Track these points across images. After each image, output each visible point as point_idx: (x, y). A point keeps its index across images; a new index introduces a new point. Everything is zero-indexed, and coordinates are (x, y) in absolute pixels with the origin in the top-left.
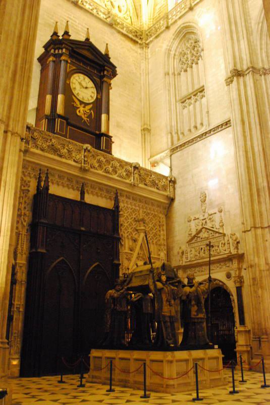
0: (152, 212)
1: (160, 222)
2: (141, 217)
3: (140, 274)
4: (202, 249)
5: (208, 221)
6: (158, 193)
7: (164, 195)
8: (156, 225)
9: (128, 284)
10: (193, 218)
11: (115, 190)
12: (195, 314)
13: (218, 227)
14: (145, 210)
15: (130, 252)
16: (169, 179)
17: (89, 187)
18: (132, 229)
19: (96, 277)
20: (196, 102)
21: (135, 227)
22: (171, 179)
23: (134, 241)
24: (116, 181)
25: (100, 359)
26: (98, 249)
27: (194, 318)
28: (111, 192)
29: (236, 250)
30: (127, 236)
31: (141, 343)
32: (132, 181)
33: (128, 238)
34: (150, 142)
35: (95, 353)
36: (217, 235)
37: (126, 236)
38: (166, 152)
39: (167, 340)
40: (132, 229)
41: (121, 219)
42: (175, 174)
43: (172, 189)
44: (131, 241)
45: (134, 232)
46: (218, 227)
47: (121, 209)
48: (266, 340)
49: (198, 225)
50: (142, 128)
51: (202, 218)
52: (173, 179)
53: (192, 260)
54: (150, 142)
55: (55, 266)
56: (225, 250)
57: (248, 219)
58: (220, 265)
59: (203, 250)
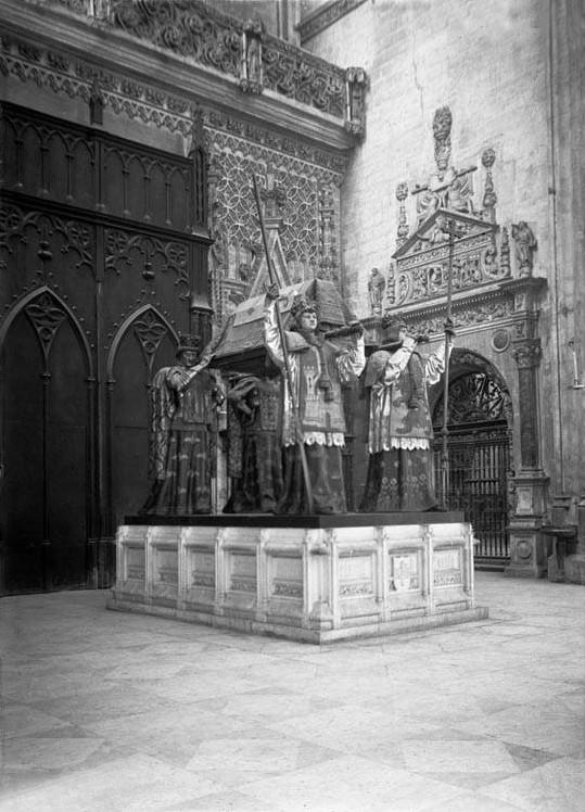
4: (432, 271)
5: (452, 195)
9: (214, 350)
10: (412, 188)
13: (479, 208)
15: (240, 281)
19: (144, 344)
23: (253, 253)
28: (182, 111)
29: (526, 269)
31: (247, 508)
36: (476, 230)
46: (479, 208)
47: (214, 162)
49: (424, 207)
51: (435, 185)
52: (361, 79)
53: (405, 302)
55: (23, 312)
56: (495, 272)
57: (568, 174)
58: (480, 312)
59: (434, 276)
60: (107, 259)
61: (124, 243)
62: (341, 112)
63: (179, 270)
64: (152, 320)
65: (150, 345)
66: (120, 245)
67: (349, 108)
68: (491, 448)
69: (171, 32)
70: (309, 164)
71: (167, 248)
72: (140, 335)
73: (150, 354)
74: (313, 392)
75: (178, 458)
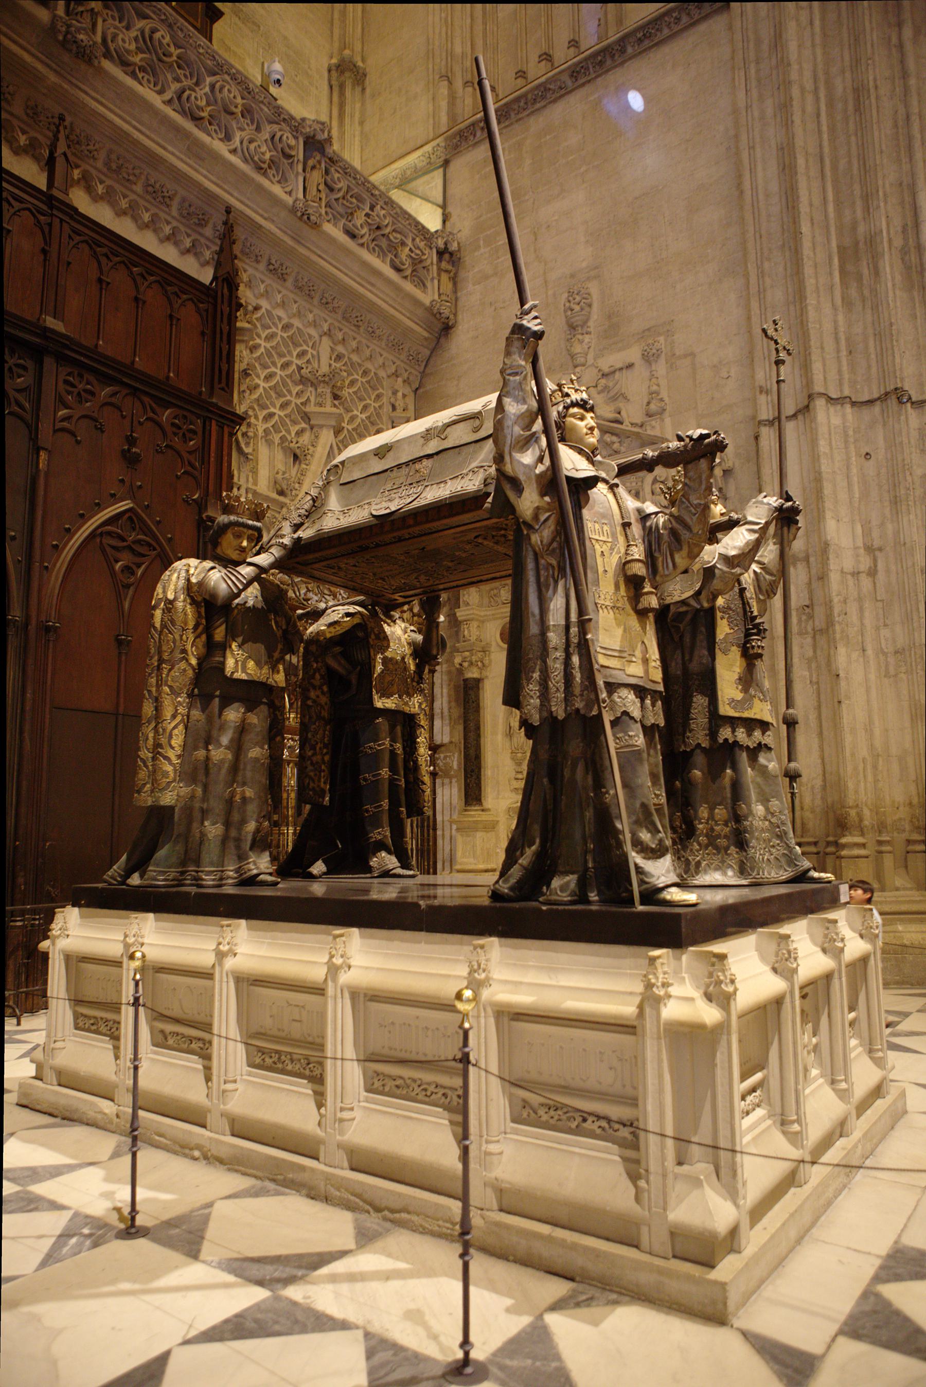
0: (368, 365)
1: (394, 408)
2: (324, 369)
3: (377, 466)
6: (398, 289)
7: (417, 302)
8: (378, 415)
9: (297, 527)
11: (218, 218)
12: (739, 696)
14: (340, 349)
15: (274, 495)
16: (440, 243)
17: (100, 164)
18: (288, 411)
21: (299, 402)
22: (446, 244)
23: (296, 457)
25: (24, 1102)
26: (131, 441)
27: (733, 722)
32: (301, 196)
33: (269, 443)
34: (361, 123)
35: (76, 932)
37: (261, 432)
38: (428, 148)
39: (639, 860)
40: (288, 411)
41: (243, 355)
42: (463, 227)
43: (447, 286)
44: (279, 456)
45: (295, 422)
48: (862, 852)
54: (361, 123)
60: (62, 413)
61: (93, 394)
62: (424, 285)
63: (186, 456)
64: (134, 529)
65: (127, 569)
67: (436, 282)
70: (378, 350)
72: (108, 549)
73: (127, 586)
74: (611, 589)
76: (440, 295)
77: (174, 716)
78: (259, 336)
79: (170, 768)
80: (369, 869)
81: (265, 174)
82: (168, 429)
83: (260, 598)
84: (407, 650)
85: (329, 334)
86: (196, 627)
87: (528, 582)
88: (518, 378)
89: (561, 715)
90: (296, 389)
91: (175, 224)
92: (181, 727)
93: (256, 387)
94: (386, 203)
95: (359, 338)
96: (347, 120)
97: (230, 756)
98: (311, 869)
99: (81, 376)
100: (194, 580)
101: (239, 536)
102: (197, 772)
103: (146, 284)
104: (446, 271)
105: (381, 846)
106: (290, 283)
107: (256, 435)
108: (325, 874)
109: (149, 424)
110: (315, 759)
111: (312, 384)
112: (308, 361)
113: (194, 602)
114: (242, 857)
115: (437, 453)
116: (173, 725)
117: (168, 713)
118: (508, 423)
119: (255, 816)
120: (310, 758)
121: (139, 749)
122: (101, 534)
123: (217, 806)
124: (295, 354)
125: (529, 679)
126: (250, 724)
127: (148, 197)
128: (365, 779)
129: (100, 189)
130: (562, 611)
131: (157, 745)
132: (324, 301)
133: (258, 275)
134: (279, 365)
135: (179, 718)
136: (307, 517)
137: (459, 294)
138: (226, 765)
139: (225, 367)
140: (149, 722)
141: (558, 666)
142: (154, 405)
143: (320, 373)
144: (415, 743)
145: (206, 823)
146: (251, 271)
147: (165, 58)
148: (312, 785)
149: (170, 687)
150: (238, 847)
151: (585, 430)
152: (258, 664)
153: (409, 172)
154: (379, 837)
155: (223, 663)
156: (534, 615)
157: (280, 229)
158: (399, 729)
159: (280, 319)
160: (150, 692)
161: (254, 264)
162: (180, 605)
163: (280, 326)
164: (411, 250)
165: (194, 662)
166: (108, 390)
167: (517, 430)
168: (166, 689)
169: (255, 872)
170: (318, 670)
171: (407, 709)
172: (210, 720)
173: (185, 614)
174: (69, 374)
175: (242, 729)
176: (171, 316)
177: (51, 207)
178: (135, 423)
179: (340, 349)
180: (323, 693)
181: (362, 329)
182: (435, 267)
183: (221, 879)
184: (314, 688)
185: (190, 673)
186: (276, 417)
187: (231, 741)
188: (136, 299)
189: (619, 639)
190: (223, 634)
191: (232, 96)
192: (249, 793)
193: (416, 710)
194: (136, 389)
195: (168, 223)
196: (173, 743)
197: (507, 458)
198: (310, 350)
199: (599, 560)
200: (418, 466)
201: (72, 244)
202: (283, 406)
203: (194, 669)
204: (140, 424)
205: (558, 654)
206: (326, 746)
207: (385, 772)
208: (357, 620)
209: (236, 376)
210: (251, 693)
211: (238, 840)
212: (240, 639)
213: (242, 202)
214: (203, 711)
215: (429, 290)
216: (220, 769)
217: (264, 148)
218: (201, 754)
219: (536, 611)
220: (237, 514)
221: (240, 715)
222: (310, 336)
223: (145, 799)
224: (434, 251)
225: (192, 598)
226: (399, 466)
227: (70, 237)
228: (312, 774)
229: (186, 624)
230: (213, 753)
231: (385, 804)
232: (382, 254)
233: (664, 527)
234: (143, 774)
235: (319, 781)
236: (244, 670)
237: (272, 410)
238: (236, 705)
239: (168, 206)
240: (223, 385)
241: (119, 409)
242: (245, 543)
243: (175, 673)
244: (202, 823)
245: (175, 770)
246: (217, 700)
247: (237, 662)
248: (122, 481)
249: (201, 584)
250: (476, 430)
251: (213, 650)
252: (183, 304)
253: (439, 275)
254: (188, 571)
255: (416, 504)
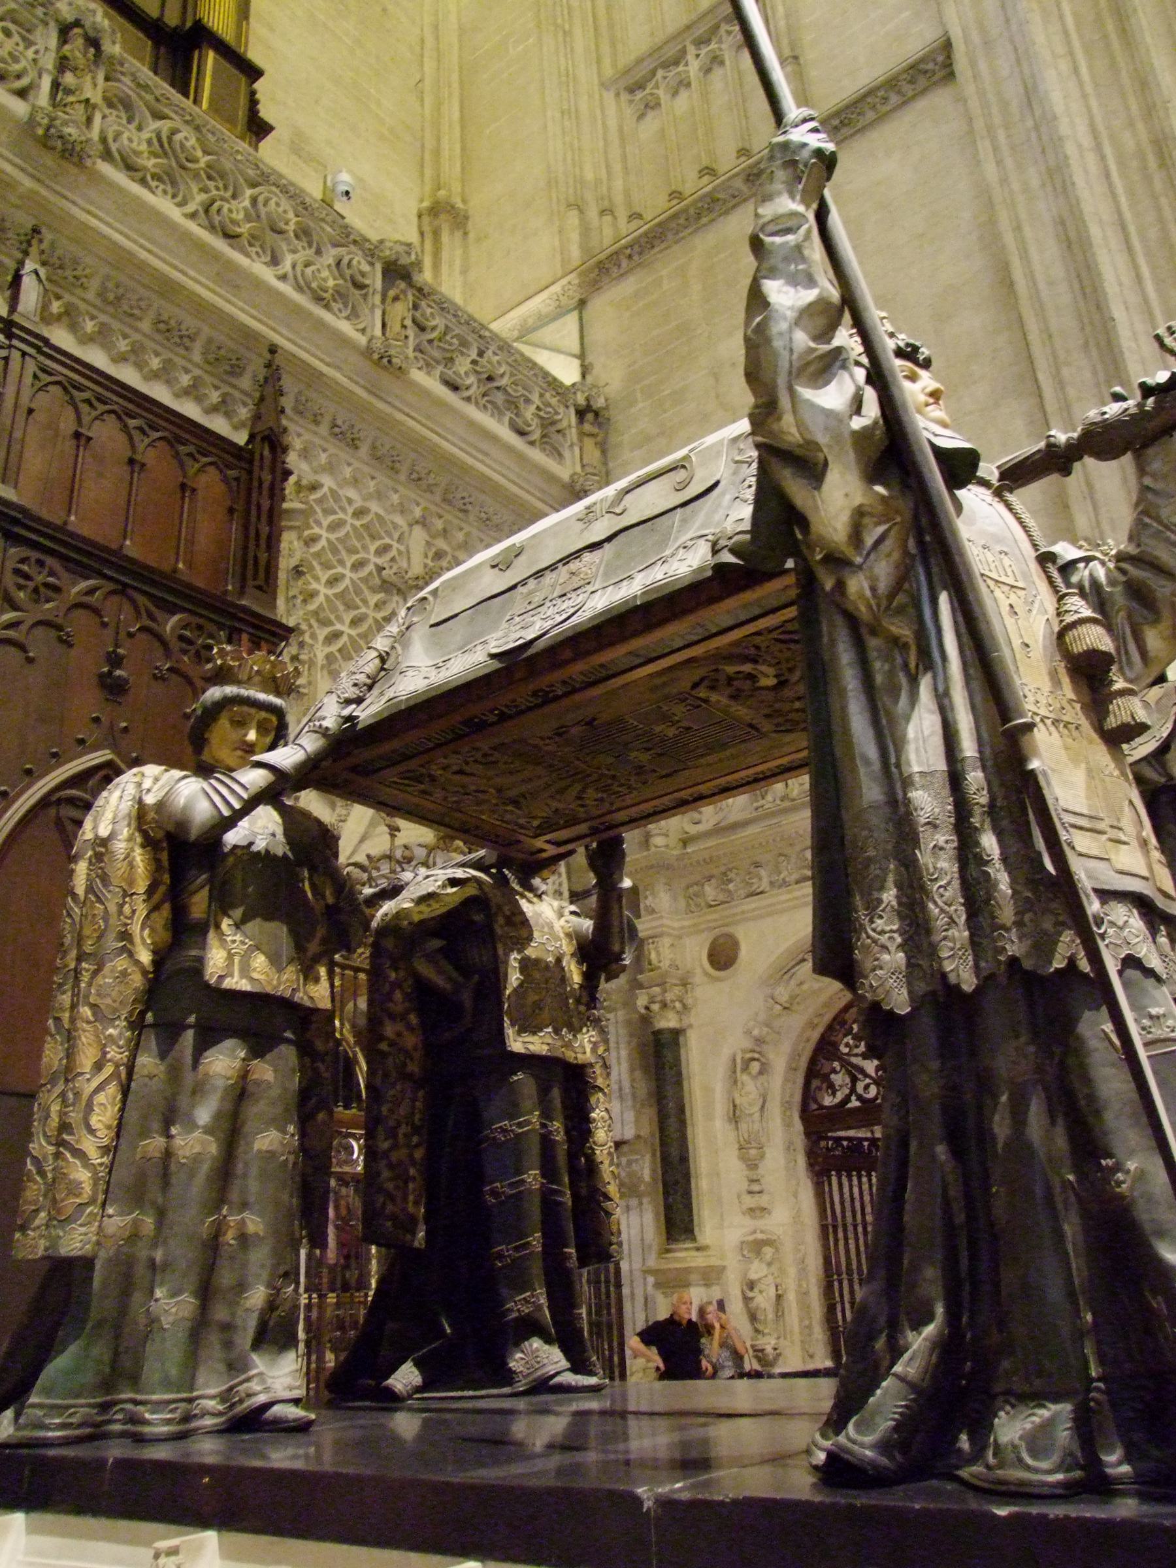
6: (521, 458)
14: (441, 544)
16: (581, 399)
20: (708, 71)
22: (587, 399)
24: (267, 294)
26: (115, 661)
30: (330, 658)
32: (378, 332)
34: (464, 272)
41: (291, 548)
42: (611, 378)
50: (426, 204)
61: (57, 589)
62: (560, 455)
66: (42, 589)
67: (577, 450)
68: (834, 1180)
69: (226, 206)
71: (171, 624)
75: (168, 1154)
76: (583, 466)
77: (98, 1066)
78: (319, 524)
79: (83, 1175)
80: (505, 1376)
81: (327, 307)
82: (175, 645)
83: (280, 837)
84: (567, 947)
85: (423, 522)
86: (151, 891)
87: (842, 693)
88: (790, 238)
89: (968, 981)
90: (373, 599)
91: (197, 372)
92: (112, 1089)
93: (313, 595)
94: (501, 348)
95: (467, 528)
96: (444, 269)
97: (213, 1148)
98: (390, 1381)
99: (41, 563)
100: (150, 800)
101: (241, 724)
102: (142, 1183)
103: (147, 441)
104: (592, 435)
105: (530, 1327)
106: (364, 450)
107: (312, 663)
108: (418, 1390)
109: (143, 636)
110: (394, 1157)
111: (399, 591)
112: (393, 559)
113: (149, 842)
114: (236, 1366)
115: (609, 539)
116: (95, 1084)
117: (86, 1059)
118: (779, 327)
119: (265, 1275)
120: (386, 1154)
121: (29, 1136)
122: (59, 801)
123: (181, 1252)
124: (373, 548)
125: (873, 906)
126: (258, 1083)
127: (158, 337)
128: (494, 1193)
129: (90, 326)
130: (936, 743)
131: (65, 1127)
132: (414, 476)
133: (318, 441)
134: (349, 565)
135: (109, 1070)
136: (370, 687)
137: (611, 465)
138: (205, 1167)
139: (263, 557)
140: (53, 1081)
141: (943, 864)
142: (153, 609)
143: (410, 575)
144: (588, 1120)
145: (158, 1293)
146: (307, 436)
147: (189, 165)
148: (390, 1208)
149: (94, 1007)
150: (228, 1345)
151: (923, 398)
152: (275, 960)
153: (530, 321)
154: (526, 1310)
155: (201, 961)
156: (867, 762)
157: (350, 378)
158: (556, 1093)
159: (350, 501)
160: (57, 1020)
161: (313, 427)
162: (120, 846)
163: (350, 511)
164: (538, 408)
165: (145, 957)
166: (84, 585)
167: (801, 339)
168: (86, 1011)
169: (262, 1399)
170: (397, 985)
171: (570, 1056)
172: (174, 1074)
173: (131, 865)
174: (23, 561)
175: (241, 1093)
176: (183, 487)
177: (10, 336)
178: (122, 635)
179: (441, 544)
180: (410, 1028)
181: (472, 518)
182: (574, 430)
183: (187, 1418)
184: (392, 1017)
185: (137, 980)
186: (345, 638)
187: (218, 1116)
188: (131, 462)
189: (1082, 792)
190: (205, 905)
191: (281, 210)
192: (255, 1224)
193: (588, 1056)
194: (125, 585)
195: (187, 371)
196: (94, 1121)
197: (784, 402)
198: (395, 544)
199: (1009, 621)
200: (574, 566)
201: (39, 384)
202: (355, 623)
203: (145, 973)
204: (131, 635)
205: (941, 838)
206: (416, 1130)
207: (533, 1178)
208: (471, 891)
209: (282, 576)
210: (258, 1019)
211: (227, 1327)
212: (238, 913)
213: (295, 344)
214: (163, 1055)
215: (568, 462)
216: (192, 1174)
217: (325, 273)
218: (156, 1143)
219: (872, 752)
220: (238, 683)
221: (237, 1064)
222: (396, 526)
223: (33, 1244)
224: (572, 411)
225: (144, 833)
226: (539, 574)
227: (35, 376)
228: (390, 1186)
229: (131, 882)
230: (178, 1142)
231: (536, 1240)
232: (497, 411)
233: (1112, 582)
234: (34, 1190)
235: (405, 1199)
236: (245, 971)
237: (338, 627)
238: (229, 1043)
239: (187, 349)
240: (260, 582)
241: (97, 612)
242: (252, 736)
243: (106, 980)
244: (152, 1292)
245: (96, 1180)
246: (190, 1034)
247: (230, 957)
248: (97, 720)
249: (161, 805)
250: (681, 487)
251: (183, 934)
252: (201, 470)
253: (581, 441)
254: (139, 784)
255: (575, 620)
